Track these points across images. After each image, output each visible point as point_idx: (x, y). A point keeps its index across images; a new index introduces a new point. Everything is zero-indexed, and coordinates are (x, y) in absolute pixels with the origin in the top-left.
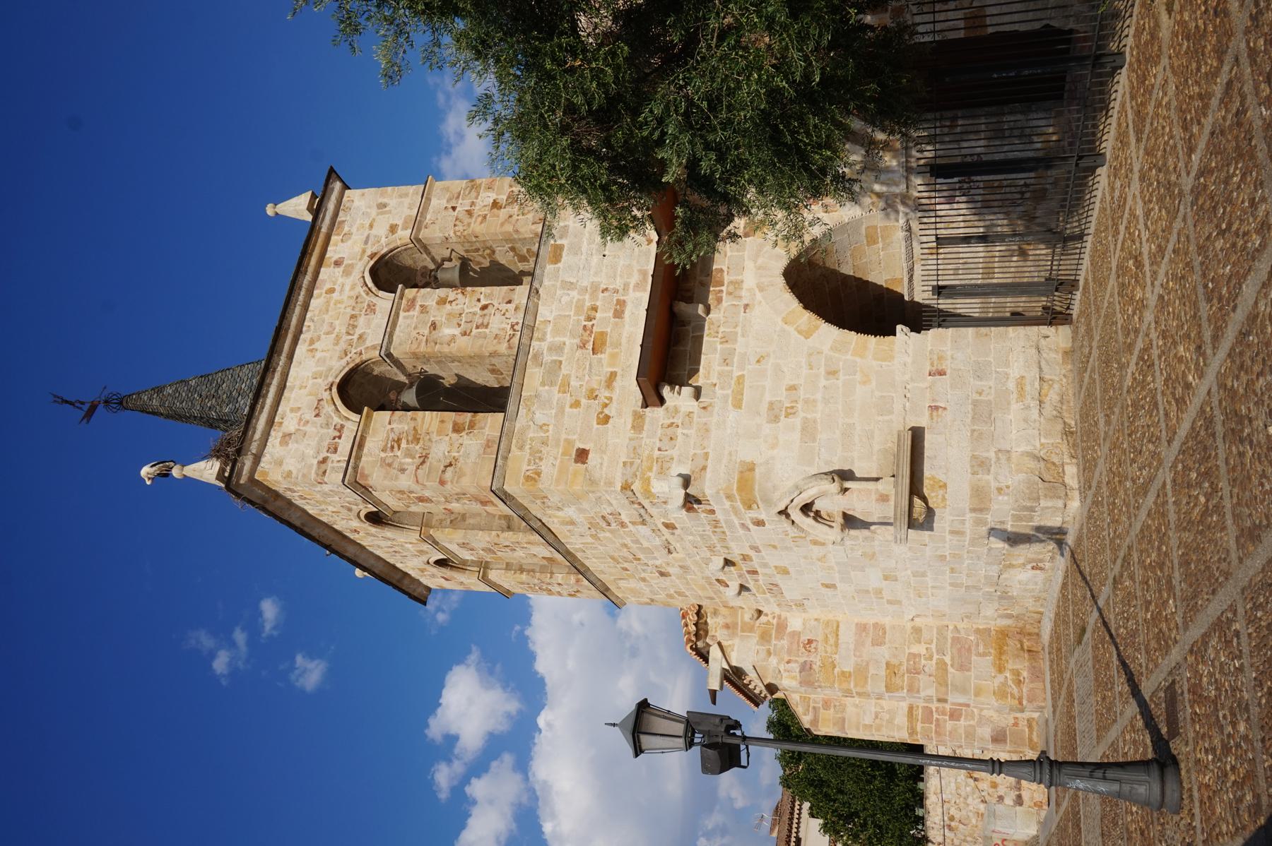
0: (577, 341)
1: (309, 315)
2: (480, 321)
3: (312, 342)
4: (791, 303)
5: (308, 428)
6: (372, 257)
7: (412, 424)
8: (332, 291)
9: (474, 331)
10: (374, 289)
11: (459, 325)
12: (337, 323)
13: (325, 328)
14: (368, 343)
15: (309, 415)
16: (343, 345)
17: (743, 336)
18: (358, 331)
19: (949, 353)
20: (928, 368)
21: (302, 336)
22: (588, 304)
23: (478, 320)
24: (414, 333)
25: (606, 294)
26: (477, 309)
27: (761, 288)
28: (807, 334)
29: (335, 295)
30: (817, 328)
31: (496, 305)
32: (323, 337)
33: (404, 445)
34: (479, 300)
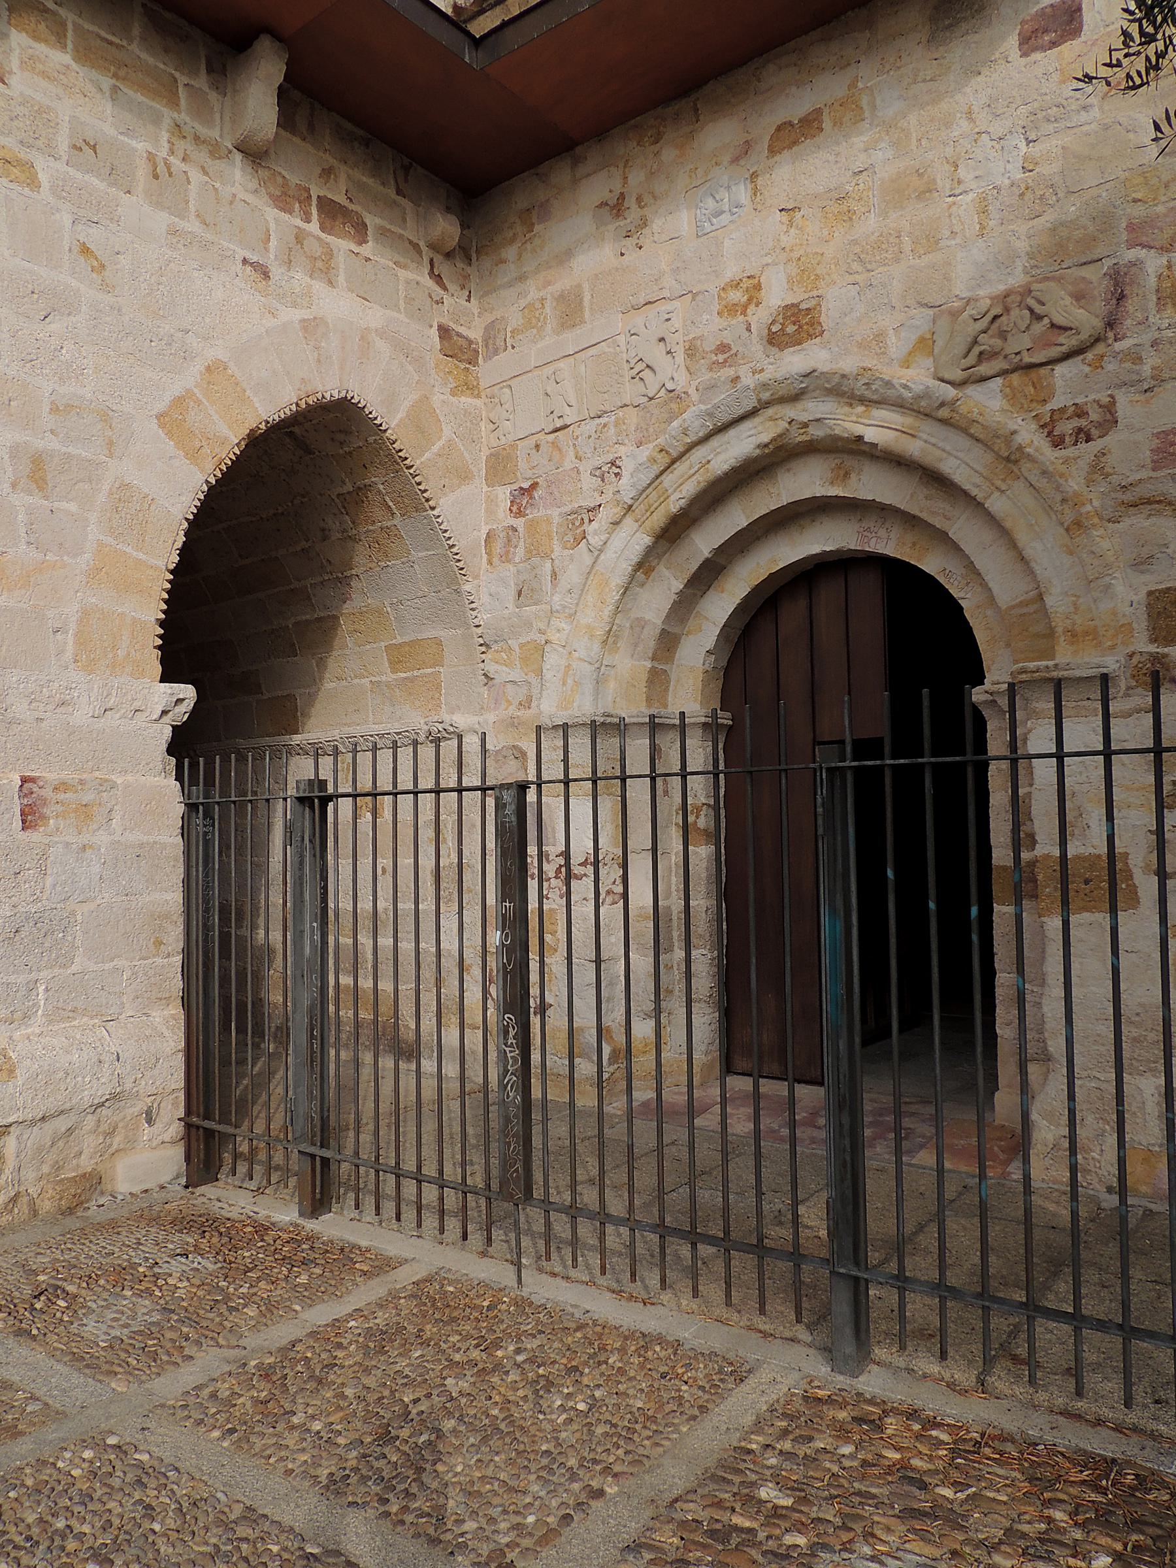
4: (270, 403)
17: (173, 232)
19: (102, 839)
20: (50, 775)
27: (310, 327)
28: (173, 420)
30: (193, 455)
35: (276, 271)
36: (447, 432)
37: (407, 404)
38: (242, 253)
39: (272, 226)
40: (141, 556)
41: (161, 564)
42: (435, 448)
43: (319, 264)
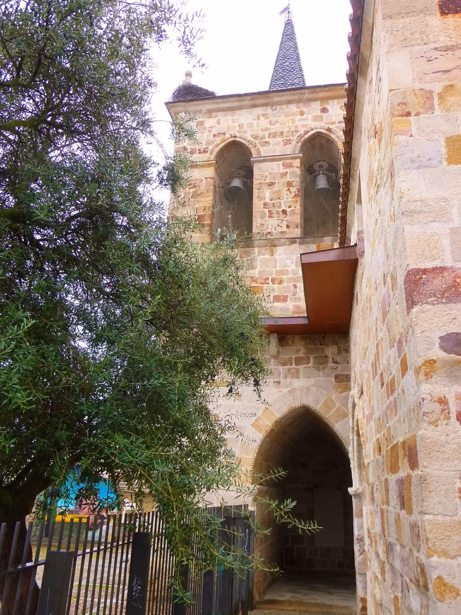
0: (257, 275)
1: (284, 106)
2: (274, 212)
3: (264, 115)
5: (206, 133)
6: (329, 130)
7: (205, 191)
8: (302, 113)
9: (267, 210)
10: (303, 139)
11: (271, 200)
12: (278, 125)
13: (274, 119)
14: (261, 149)
15: (214, 131)
16: (260, 133)
18: (271, 140)
21: (269, 108)
22: (285, 277)
23: (274, 210)
24: (267, 174)
25: (292, 288)
26: (283, 208)
29: (299, 117)
30: (260, 431)
31: (286, 219)
32: (268, 120)
33: (192, 190)
34: (290, 207)
35: (283, 381)
36: (338, 405)
37: (323, 401)
38: (273, 381)
39: (281, 371)
40: (247, 456)
41: (252, 457)
42: (333, 411)
43: (295, 374)
